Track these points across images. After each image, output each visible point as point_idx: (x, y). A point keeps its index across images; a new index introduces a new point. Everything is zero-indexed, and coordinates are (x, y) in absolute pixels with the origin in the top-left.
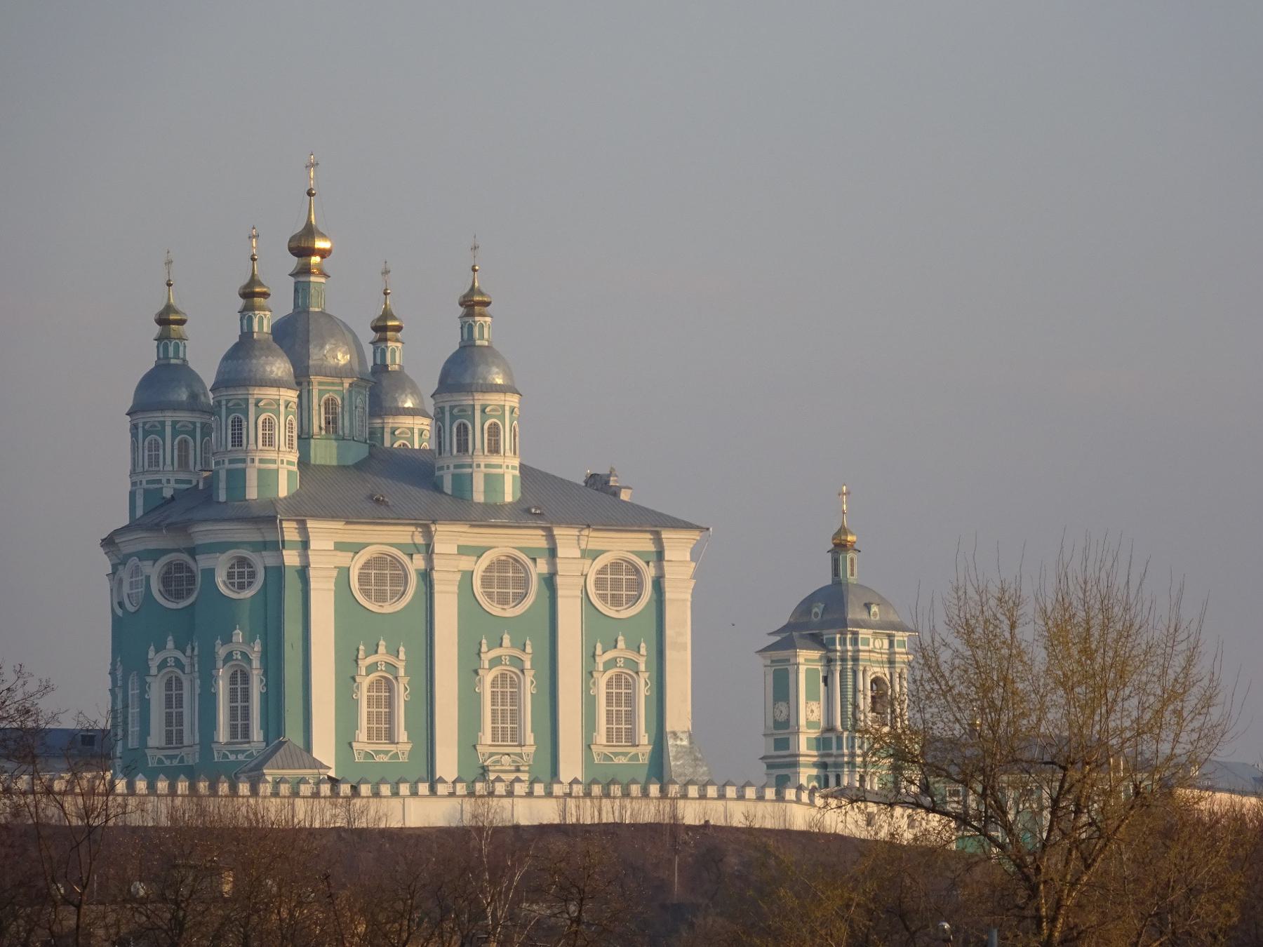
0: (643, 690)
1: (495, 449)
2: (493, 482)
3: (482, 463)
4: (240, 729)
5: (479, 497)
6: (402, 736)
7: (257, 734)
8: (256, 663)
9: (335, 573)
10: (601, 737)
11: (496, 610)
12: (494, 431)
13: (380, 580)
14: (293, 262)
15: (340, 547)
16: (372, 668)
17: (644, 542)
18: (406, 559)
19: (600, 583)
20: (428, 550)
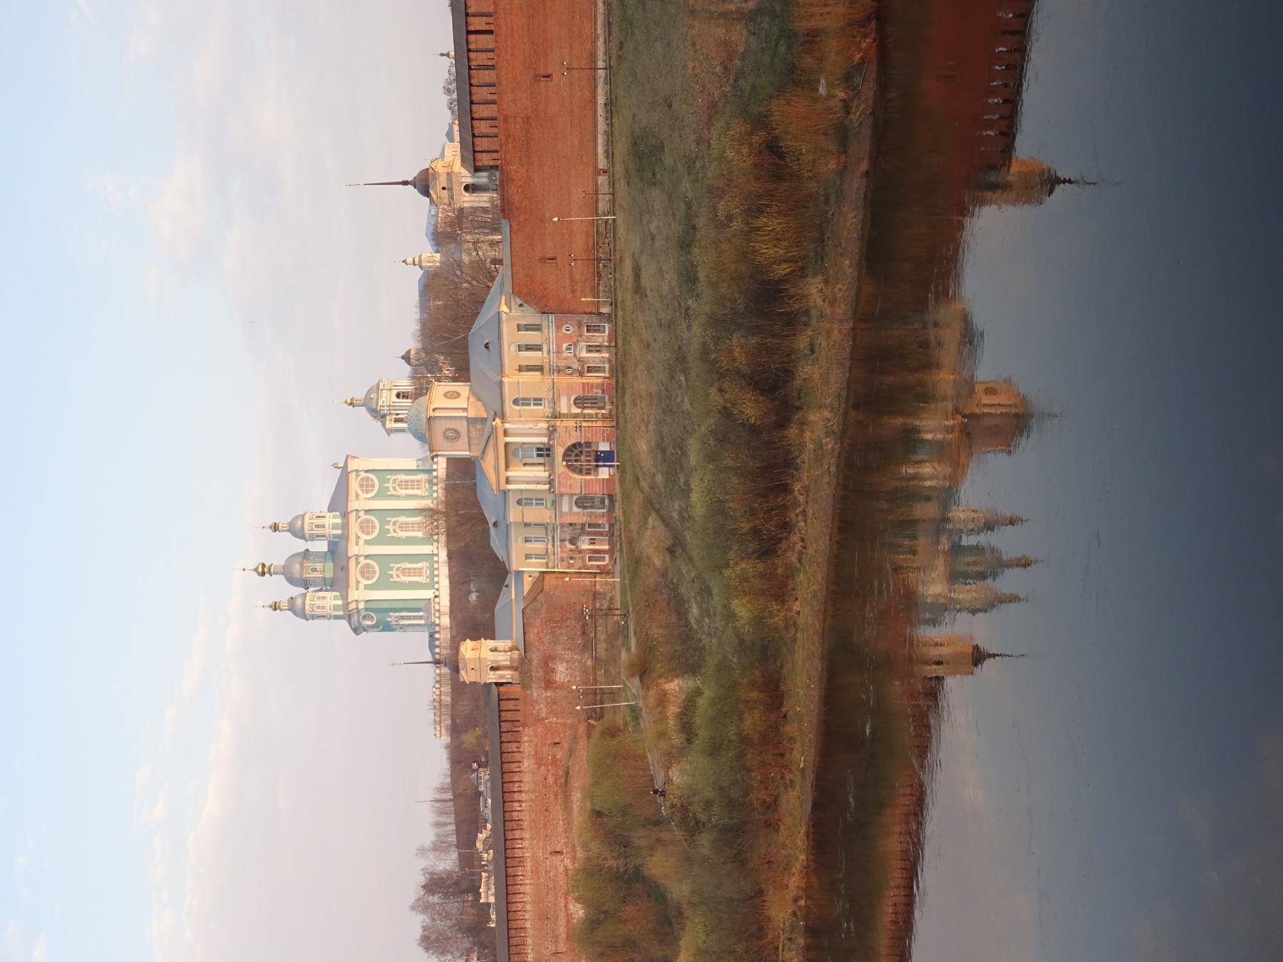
0: (403, 477)
1: (323, 526)
2: (335, 526)
3: (329, 531)
4: (420, 618)
5: (339, 532)
6: (420, 565)
7: (421, 614)
8: (398, 614)
9: (366, 591)
10: (419, 492)
11: (377, 531)
12: (317, 526)
13: (368, 572)
14: (267, 575)
15: (357, 589)
16: (398, 576)
17: (352, 476)
18: (361, 564)
19: (367, 492)
20: (357, 556)
